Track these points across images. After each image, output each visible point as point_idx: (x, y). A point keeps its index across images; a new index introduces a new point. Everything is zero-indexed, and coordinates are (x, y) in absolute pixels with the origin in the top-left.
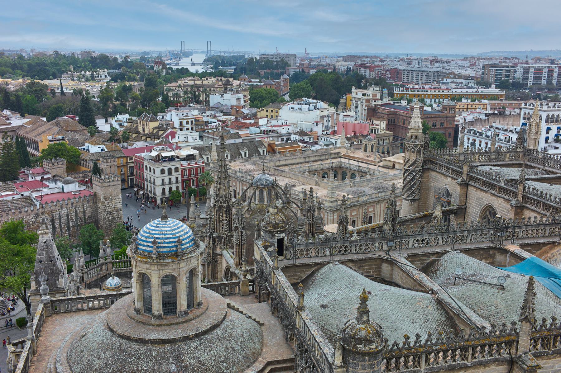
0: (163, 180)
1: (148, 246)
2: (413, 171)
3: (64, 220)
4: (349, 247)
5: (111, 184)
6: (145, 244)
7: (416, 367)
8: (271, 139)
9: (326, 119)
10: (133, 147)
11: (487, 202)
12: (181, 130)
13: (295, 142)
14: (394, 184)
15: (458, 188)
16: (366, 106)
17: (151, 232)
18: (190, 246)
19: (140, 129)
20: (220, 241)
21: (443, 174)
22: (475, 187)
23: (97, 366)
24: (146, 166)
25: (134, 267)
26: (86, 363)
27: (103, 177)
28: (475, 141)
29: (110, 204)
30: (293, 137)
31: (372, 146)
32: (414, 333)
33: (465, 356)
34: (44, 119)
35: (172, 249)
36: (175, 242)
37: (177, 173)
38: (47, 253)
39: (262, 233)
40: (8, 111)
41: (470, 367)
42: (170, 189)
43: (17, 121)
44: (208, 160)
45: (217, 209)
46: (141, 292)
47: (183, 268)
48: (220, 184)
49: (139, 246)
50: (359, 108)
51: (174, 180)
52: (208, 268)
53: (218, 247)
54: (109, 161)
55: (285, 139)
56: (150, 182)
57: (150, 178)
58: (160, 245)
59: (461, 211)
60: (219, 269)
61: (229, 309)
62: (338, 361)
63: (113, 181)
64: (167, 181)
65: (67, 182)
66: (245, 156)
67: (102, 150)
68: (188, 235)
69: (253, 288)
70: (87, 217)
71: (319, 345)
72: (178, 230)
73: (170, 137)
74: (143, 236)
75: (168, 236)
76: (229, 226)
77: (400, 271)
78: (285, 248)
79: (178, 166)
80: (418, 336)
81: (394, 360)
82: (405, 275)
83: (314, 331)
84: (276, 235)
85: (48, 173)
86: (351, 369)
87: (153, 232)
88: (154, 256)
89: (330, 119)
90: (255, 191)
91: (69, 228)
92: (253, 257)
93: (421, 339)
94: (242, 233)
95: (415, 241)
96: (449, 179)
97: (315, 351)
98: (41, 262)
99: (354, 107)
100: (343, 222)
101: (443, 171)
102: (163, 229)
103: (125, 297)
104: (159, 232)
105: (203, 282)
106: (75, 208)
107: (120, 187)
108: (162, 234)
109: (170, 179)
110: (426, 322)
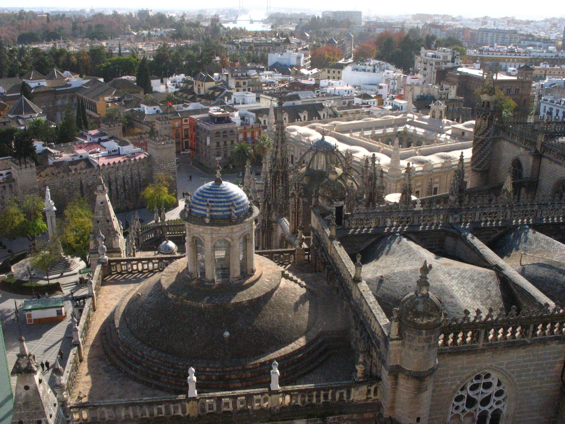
0: (218, 143)
1: (202, 210)
2: (483, 140)
3: (120, 182)
4: (412, 219)
5: (166, 146)
6: (199, 207)
7: (474, 342)
8: (332, 101)
9: (391, 81)
10: (188, 109)
11: (561, 176)
12: (238, 91)
13: (358, 106)
14: (462, 153)
15: (531, 159)
16: (436, 68)
17: (205, 195)
19: (196, 89)
20: (276, 207)
21: (515, 144)
22: (549, 158)
23: (153, 325)
25: (187, 230)
26: (142, 322)
27: (157, 139)
28: (551, 109)
29: (165, 167)
30: (358, 101)
31: (441, 112)
32: (474, 309)
33: (525, 333)
34: (102, 80)
35: (225, 213)
36: (229, 206)
38: (104, 215)
39: (320, 200)
40: (68, 72)
41: (530, 344)
43: (75, 81)
44: (265, 123)
46: (195, 256)
47: (236, 232)
48: (277, 147)
49: (193, 210)
50: (428, 71)
52: (263, 235)
53: (274, 214)
54: (163, 122)
55: (347, 101)
58: (213, 209)
59: (532, 185)
60: (274, 236)
62: (394, 332)
63: (167, 143)
64: (222, 144)
65: (123, 143)
66: (304, 119)
67: (157, 111)
68: (242, 199)
70: (141, 180)
71: (375, 317)
73: (226, 98)
75: (222, 200)
77: (464, 245)
78: (343, 216)
80: (478, 312)
81: (452, 335)
82: (469, 250)
83: (371, 303)
84: (335, 202)
85: (105, 135)
86: (407, 342)
87: (207, 195)
88: (207, 220)
89: (396, 81)
90: (313, 157)
91: (125, 190)
93: (482, 314)
94: (299, 200)
95: (482, 215)
96: (522, 150)
97: (370, 324)
98: (98, 222)
99: (422, 70)
100: (406, 192)
101: (516, 141)
103: (178, 260)
104: (213, 196)
105: (257, 248)
106: (131, 171)
107: (174, 149)
108: (216, 198)
109: (225, 142)
110: (488, 298)
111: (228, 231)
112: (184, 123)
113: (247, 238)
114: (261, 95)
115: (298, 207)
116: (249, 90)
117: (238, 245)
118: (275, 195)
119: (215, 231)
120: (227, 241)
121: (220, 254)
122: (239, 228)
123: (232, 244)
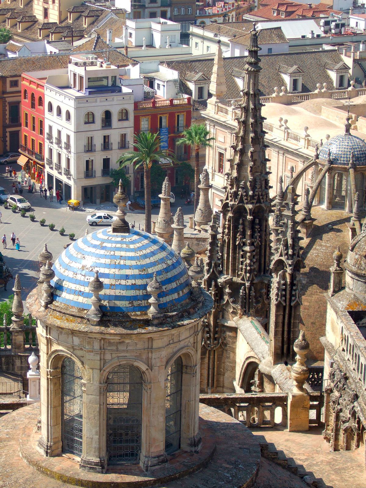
18: (179, 300)
24: (50, 105)
35: (136, 303)
36: (144, 287)
37: (125, 124)
42: (106, 162)
45: (230, 215)
46: (58, 402)
51: (115, 140)
56: (59, 142)
57: (59, 132)
61: (263, 460)
64: (98, 142)
69: (319, 415)
72: (152, 259)
74: (67, 267)
75: (129, 272)
76: (259, 261)
79: (126, 107)
92: (322, 339)
102: (118, 253)
103: (14, 414)
108: (115, 266)
111: (140, 346)
112: (9, 89)
113: (184, 363)
114: (193, 29)
115: (291, 295)
116: (164, 16)
117: (162, 379)
118: (234, 265)
119: (110, 344)
120: (138, 368)
121: (119, 399)
122: (166, 340)
123: (149, 375)
